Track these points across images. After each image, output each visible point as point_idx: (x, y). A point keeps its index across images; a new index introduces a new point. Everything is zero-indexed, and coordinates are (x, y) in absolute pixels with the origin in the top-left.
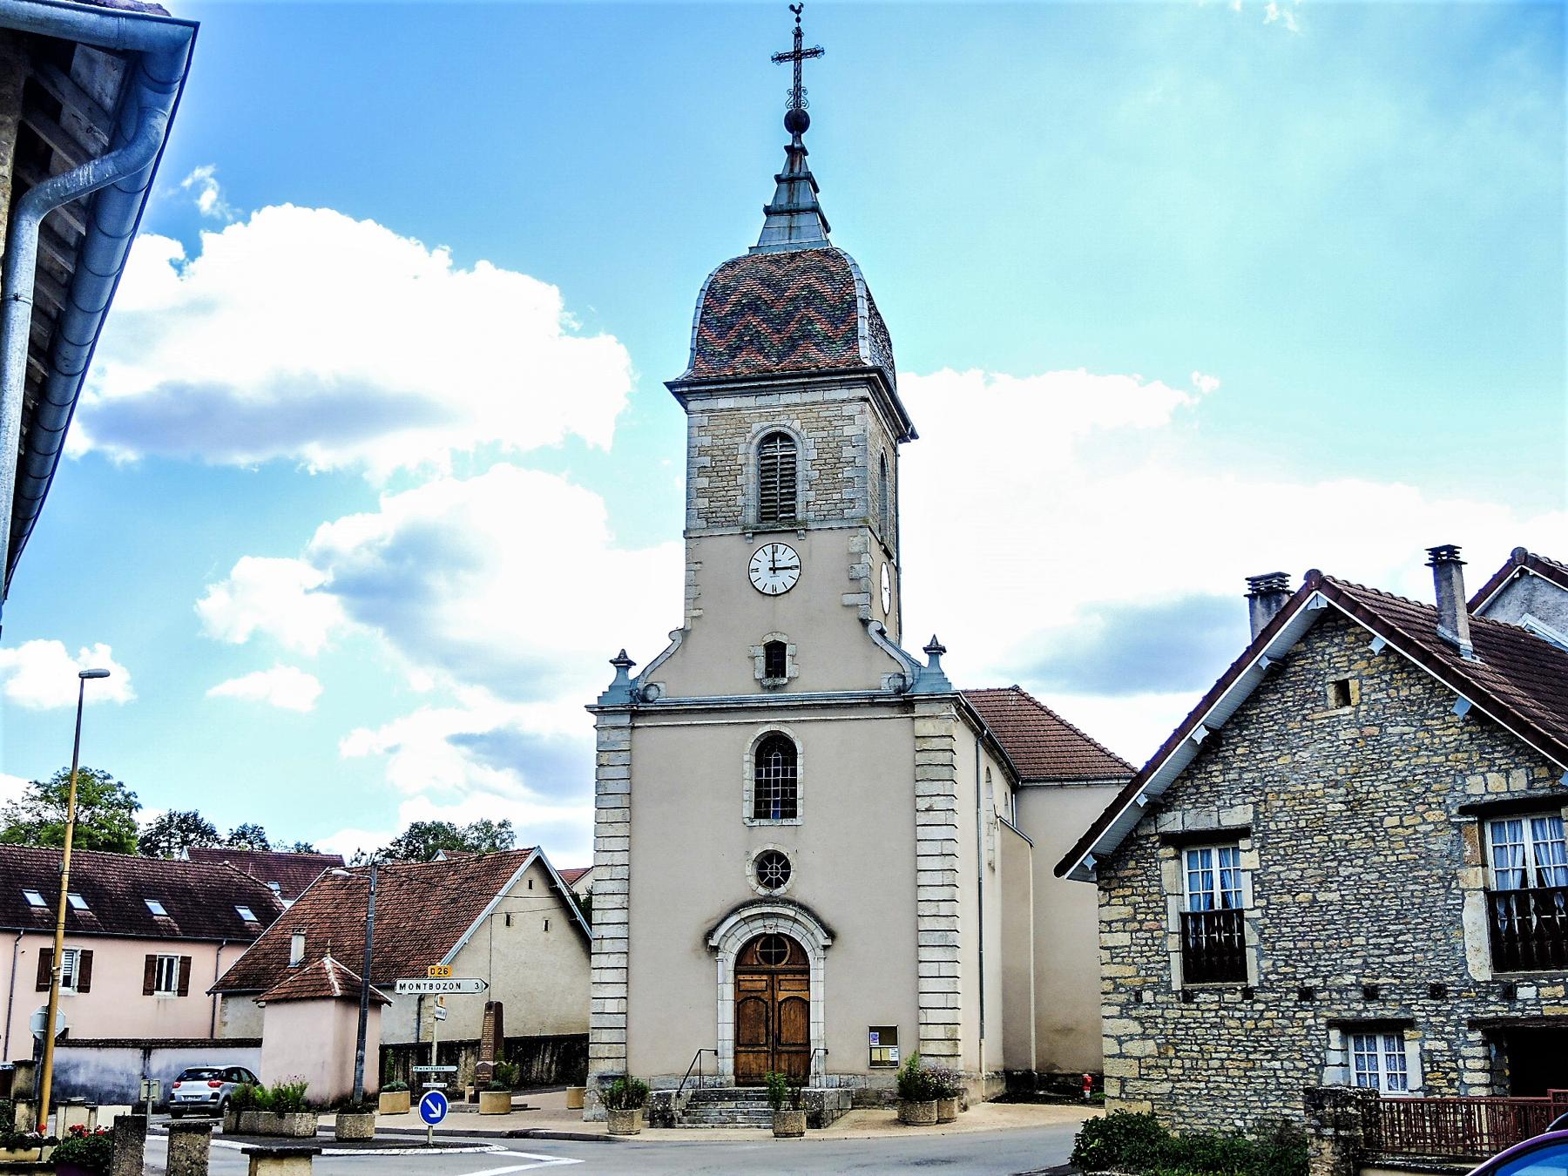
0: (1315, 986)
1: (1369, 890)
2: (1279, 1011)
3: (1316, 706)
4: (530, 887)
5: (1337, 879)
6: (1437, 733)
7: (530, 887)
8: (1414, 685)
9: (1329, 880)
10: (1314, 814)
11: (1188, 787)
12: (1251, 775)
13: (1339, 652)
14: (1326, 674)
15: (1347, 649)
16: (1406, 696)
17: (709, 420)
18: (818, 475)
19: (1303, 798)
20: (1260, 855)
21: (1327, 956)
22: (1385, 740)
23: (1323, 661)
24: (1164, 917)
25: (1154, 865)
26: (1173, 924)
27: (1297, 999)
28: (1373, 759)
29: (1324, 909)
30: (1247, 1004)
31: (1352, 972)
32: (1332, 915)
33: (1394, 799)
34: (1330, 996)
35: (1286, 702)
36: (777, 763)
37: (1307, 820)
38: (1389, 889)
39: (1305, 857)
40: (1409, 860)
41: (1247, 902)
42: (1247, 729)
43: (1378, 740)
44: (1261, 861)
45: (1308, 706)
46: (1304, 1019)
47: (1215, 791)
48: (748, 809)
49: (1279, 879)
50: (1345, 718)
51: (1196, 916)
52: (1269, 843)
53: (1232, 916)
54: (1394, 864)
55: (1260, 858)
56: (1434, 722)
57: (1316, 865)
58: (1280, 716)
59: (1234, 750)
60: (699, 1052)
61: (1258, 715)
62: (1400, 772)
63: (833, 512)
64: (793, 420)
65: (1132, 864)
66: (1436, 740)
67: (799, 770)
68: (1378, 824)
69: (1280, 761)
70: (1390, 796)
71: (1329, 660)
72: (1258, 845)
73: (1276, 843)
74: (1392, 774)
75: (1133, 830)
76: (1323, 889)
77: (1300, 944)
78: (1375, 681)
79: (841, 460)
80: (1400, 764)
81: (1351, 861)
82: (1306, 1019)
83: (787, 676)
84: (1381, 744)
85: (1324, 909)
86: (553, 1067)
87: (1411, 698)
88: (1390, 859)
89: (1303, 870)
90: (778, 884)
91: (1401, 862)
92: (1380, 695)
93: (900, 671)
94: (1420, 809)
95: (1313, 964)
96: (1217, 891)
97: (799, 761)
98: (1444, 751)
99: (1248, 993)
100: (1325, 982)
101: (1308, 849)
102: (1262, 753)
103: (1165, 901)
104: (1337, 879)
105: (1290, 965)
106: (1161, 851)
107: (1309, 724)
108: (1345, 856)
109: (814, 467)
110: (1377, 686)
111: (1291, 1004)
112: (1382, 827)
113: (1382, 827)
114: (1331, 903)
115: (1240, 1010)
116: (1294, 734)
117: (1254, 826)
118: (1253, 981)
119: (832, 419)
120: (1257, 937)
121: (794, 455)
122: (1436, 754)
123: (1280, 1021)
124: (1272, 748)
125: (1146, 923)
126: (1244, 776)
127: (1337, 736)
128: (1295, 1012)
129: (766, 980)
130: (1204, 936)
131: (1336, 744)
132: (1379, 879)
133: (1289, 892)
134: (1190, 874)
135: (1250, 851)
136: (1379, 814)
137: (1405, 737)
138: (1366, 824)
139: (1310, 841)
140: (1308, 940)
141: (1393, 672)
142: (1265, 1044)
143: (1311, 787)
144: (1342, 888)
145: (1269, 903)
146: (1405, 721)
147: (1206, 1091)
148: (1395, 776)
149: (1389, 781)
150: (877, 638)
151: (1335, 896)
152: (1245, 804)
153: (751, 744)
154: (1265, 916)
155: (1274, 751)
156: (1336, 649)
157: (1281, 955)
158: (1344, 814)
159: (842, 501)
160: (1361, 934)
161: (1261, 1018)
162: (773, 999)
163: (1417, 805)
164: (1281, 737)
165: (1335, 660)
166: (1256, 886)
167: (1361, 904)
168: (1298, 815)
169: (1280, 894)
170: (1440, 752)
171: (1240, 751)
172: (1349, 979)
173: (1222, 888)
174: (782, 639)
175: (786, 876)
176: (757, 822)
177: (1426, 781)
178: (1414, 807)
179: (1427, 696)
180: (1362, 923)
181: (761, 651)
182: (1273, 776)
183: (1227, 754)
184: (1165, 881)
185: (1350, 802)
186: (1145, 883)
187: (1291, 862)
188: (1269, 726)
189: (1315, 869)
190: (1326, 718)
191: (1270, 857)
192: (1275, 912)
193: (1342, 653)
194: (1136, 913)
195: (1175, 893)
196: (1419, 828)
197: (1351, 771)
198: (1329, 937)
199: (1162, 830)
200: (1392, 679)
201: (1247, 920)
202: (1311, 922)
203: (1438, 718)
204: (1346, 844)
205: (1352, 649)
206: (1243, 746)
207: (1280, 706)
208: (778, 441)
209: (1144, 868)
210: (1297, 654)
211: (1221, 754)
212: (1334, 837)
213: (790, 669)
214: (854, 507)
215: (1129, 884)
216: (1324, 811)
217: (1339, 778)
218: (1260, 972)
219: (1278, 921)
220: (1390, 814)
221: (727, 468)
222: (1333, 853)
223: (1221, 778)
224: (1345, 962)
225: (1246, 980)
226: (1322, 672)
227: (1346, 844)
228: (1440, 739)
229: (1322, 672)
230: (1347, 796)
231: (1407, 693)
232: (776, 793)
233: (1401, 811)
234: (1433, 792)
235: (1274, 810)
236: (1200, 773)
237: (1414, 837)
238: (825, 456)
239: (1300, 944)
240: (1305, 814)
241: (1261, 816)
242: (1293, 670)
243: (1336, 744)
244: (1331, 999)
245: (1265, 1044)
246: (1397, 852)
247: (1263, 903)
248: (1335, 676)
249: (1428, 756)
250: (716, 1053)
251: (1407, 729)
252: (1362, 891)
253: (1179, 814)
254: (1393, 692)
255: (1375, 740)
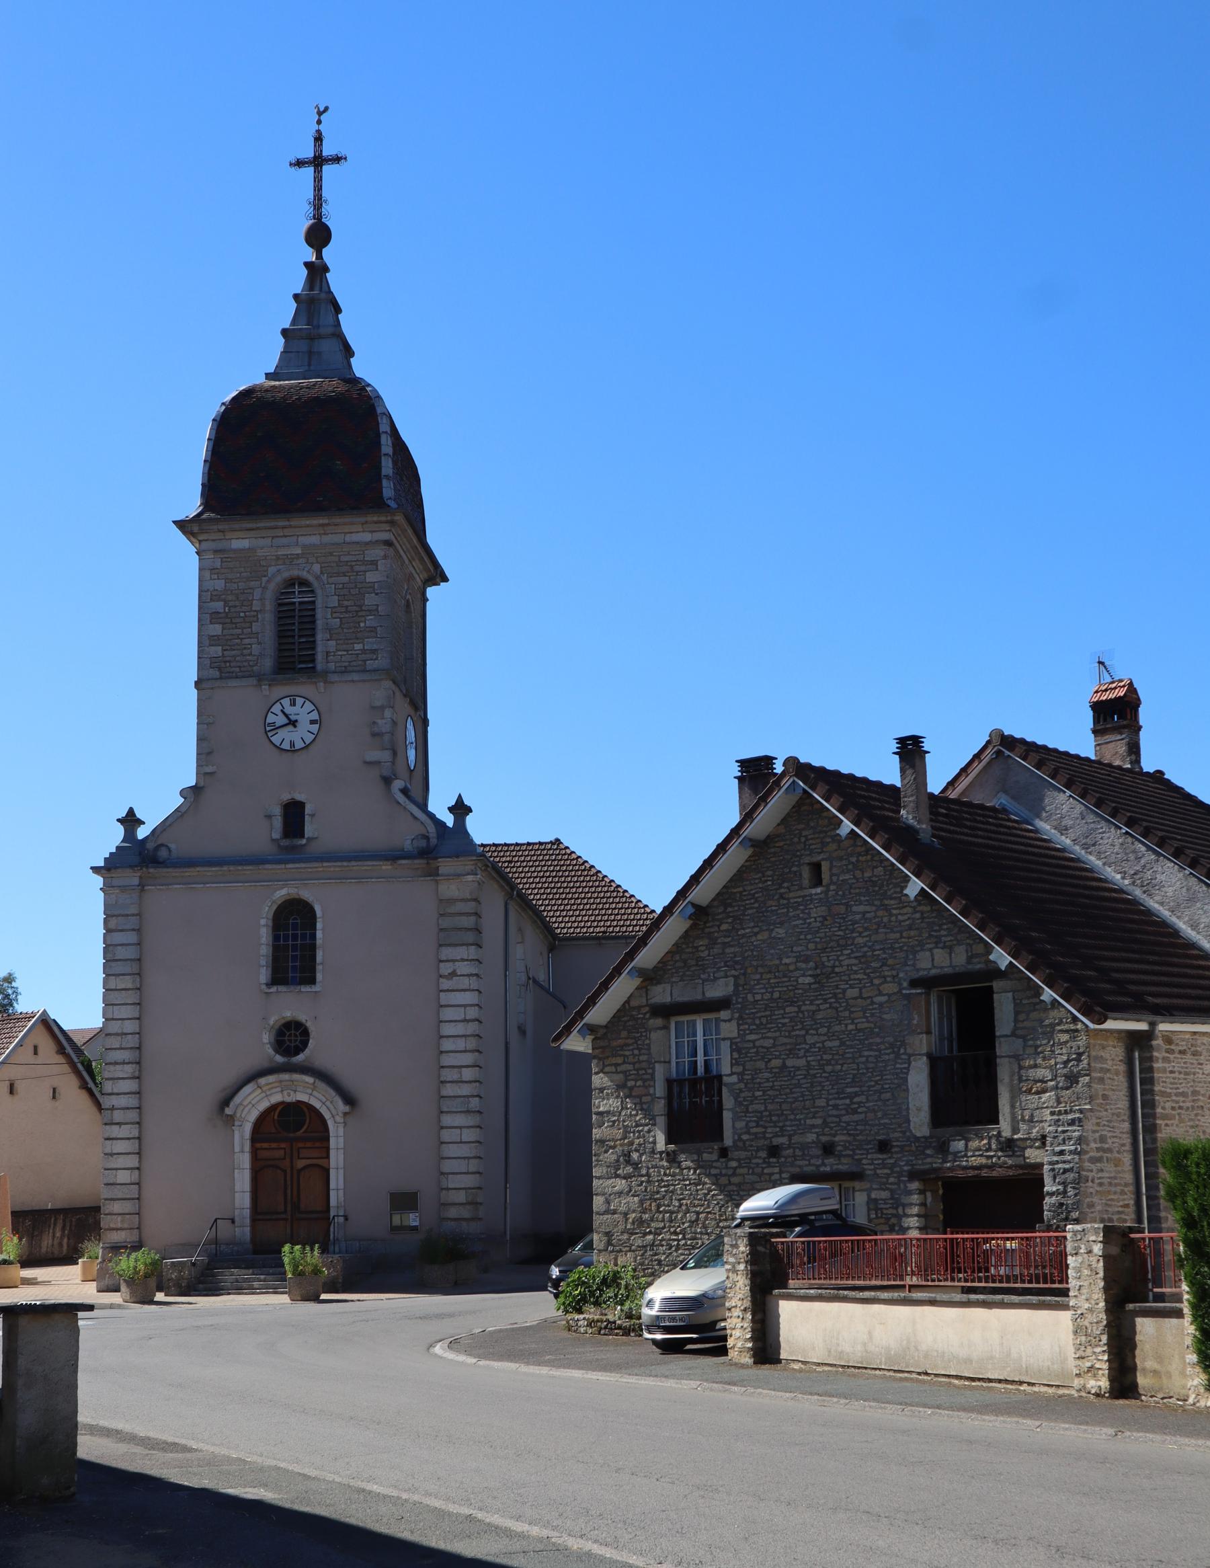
0: (782, 1144)
1: (831, 1057)
2: (749, 1168)
3: (793, 885)
4: (36, 1053)
5: (804, 1046)
6: (894, 912)
7: (36, 1053)
8: (876, 867)
9: (798, 1047)
10: (787, 986)
11: (676, 961)
12: (732, 950)
13: (814, 834)
14: (802, 855)
15: (821, 832)
16: (870, 877)
17: (222, 562)
18: (339, 624)
19: (778, 971)
20: (739, 1025)
21: (792, 1117)
22: (850, 918)
23: (799, 842)
24: (652, 1083)
25: (644, 1034)
26: (660, 1089)
27: (765, 1156)
28: (839, 936)
29: (792, 1074)
30: (722, 1163)
31: (813, 1131)
32: (799, 1080)
33: (856, 972)
34: (794, 1152)
35: (766, 881)
36: (295, 927)
37: (780, 992)
38: (847, 1055)
39: (777, 1027)
40: (866, 1028)
41: (726, 1069)
42: (731, 905)
43: (844, 918)
44: (739, 1030)
45: (785, 885)
46: (771, 1174)
47: (702, 965)
48: (264, 975)
49: (754, 1047)
50: (816, 897)
51: (680, 1082)
52: (747, 1014)
53: (713, 1081)
54: (853, 1032)
55: (738, 1028)
56: (892, 902)
57: (787, 1034)
58: (761, 894)
59: (719, 926)
60: (216, 1220)
61: (740, 893)
62: (861, 947)
63: (354, 664)
64: (312, 563)
65: (624, 1034)
66: (893, 919)
67: (319, 934)
68: (841, 996)
69: (759, 937)
70: (852, 970)
71: (805, 842)
72: (737, 1015)
73: (752, 1013)
74: (855, 950)
75: (626, 1002)
76: (792, 1056)
77: (770, 1107)
78: (844, 862)
79: (363, 608)
80: (860, 940)
81: (817, 1029)
82: (773, 1174)
83: (306, 836)
84: (847, 922)
85: (792, 1074)
86: (65, 1240)
87: (874, 879)
88: (850, 1027)
89: (775, 1039)
90: (298, 1050)
91: (859, 1030)
92: (847, 877)
93: (424, 832)
94: (876, 982)
95: (781, 1124)
96: (700, 1058)
97: (319, 925)
98: (899, 929)
99: (724, 1152)
100: (790, 1140)
101: (780, 1018)
102: (744, 929)
103: (653, 1069)
104: (804, 1046)
105: (762, 1126)
106: (651, 1021)
107: (785, 902)
108: (812, 1025)
109: (334, 615)
110: (845, 867)
111: (760, 1161)
112: (844, 998)
113: (844, 998)
114: (798, 1069)
115: (716, 1168)
116: (772, 911)
117: (734, 998)
118: (728, 1141)
119: (354, 563)
120: (733, 1101)
121: (313, 602)
122: (892, 931)
123: (750, 1177)
124: (752, 924)
125: (636, 1089)
126: (727, 950)
127: (809, 914)
128: (763, 1168)
129: (285, 1149)
130: (688, 1100)
131: (808, 921)
132: (840, 1046)
133: (763, 1058)
134: (676, 1042)
135: (729, 1021)
136: (842, 987)
137: (868, 915)
138: (831, 995)
139: (782, 1012)
140: (777, 1102)
141: (859, 854)
142: (736, 1197)
143: (786, 961)
144: (808, 1054)
145: (744, 1069)
146: (867, 900)
147: (683, 1242)
148: (857, 951)
149: (852, 955)
150: (401, 798)
151: (801, 1062)
152: (726, 976)
153: (267, 908)
154: (740, 1081)
155: (753, 927)
156: (811, 831)
157: (753, 1117)
158: (812, 986)
159: (364, 651)
160: (823, 1096)
161: (734, 1174)
162: (292, 1167)
163: (875, 978)
164: (761, 914)
165: (811, 842)
166: (734, 1053)
167: (823, 1069)
168: (773, 987)
169: (755, 1061)
170: (895, 929)
171: (724, 927)
172: (811, 1137)
173: (705, 1056)
174: (299, 797)
175: (305, 1044)
176: (274, 989)
177: (884, 956)
178: (872, 980)
179: (887, 877)
180: (824, 1086)
181: (277, 811)
182: (752, 951)
183: (712, 930)
184: (654, 1049)
185: (818, 975)
186: (636, 1052)
187: (765, 1031)
188: (751, 904)
189: (786, 1037)
190: (799, 897)
191: (747, 1026)
192: (750, 1077)
193: (817, 836)
194: (626, 1080)
195: (662, 1060)
196: (875, 1000)
197: (819, 946)
198: (796, 1100)
199: (653, 1001)
200: (858, 861)
201: (726, 1085)
202: (781, 1086)
203: (895, 898)
204: (813, 1014)
205: (826, 832)
206: (727, 923)
207: (760, 885)
208: (297, 587)
209: (634, 1038)
210: (778, 836)
211: (707, 930)
212: (803, 1008)
213: (309, 830)
214: (376, 659)
215: (622, 1053)
216: (795, 983)
217: (809, 953)
218: (734, 1133)
219: (752, 1086)
220: (852, 987)
221: (242, 614)
222: (802, 1023)
223: (707, 952)
224: (809, 1122)
225: (722, 1140)
226: (798, 853)
227: (813, 1014)
228: (897, 918)
229: (798, 853)
230: (816, 969)
231: (870, 874)
232: (294, 958)
233: (860, 983)
234: (889, 966)
235: (752, 983)
236: (688, 947)
237: (871, 1007)
238: (346, 603)
239: (770, 1107)
240: (778, 987)
241: (741, 989)
242: (773, 850)
243: (808, 921)
244: (794, 1156)
245: (736, 1197)
246: (856, 1021)
247: (740, 1069)
248: (809, 858)
249: (886, 933)
250: (233, 1221)
251: (868, 908)
252: (825, 1057)
253: (668, 987)
254: (858, 874)
255: (840, 918)
